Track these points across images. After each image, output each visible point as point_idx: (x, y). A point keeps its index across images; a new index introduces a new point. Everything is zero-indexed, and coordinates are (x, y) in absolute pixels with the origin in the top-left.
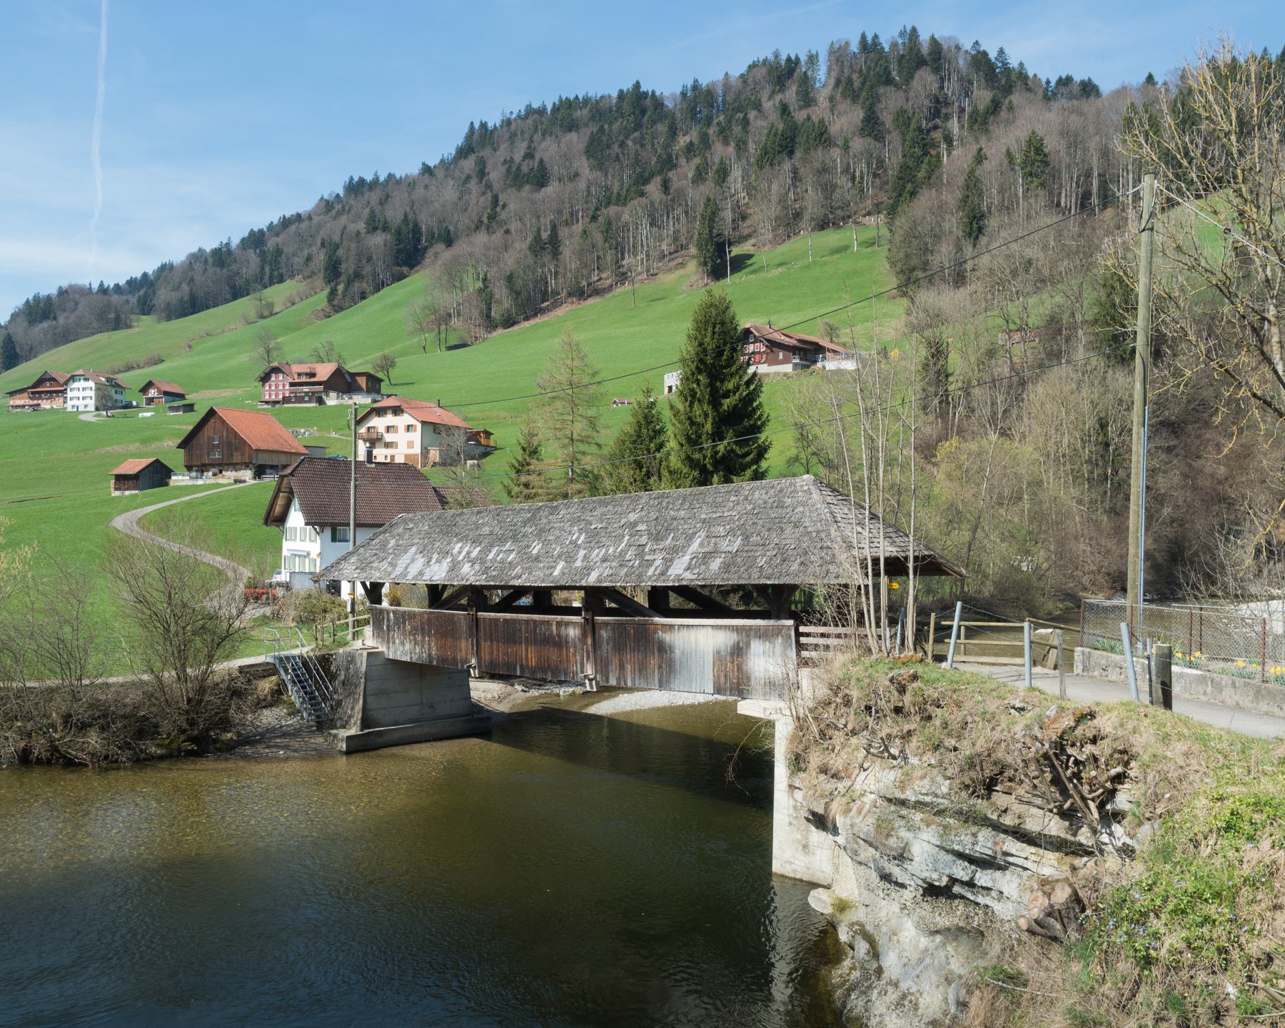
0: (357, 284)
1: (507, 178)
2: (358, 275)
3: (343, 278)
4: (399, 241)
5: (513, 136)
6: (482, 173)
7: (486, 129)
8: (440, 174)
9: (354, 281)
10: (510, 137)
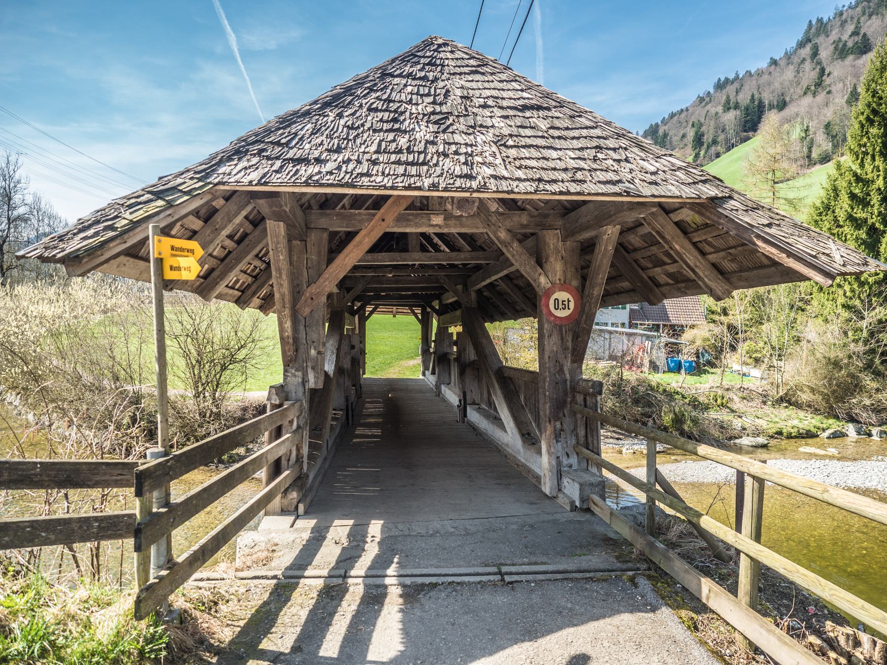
0: (713, 148)
1: (834, 53)
2: (715, 142)
3: (705, 146)
4: (747, 115)
5: (843, 24)
6: (815, 53)
7: (822, 23)
8: (783, 63)
9: (711, 146)
10: (841, 24)
